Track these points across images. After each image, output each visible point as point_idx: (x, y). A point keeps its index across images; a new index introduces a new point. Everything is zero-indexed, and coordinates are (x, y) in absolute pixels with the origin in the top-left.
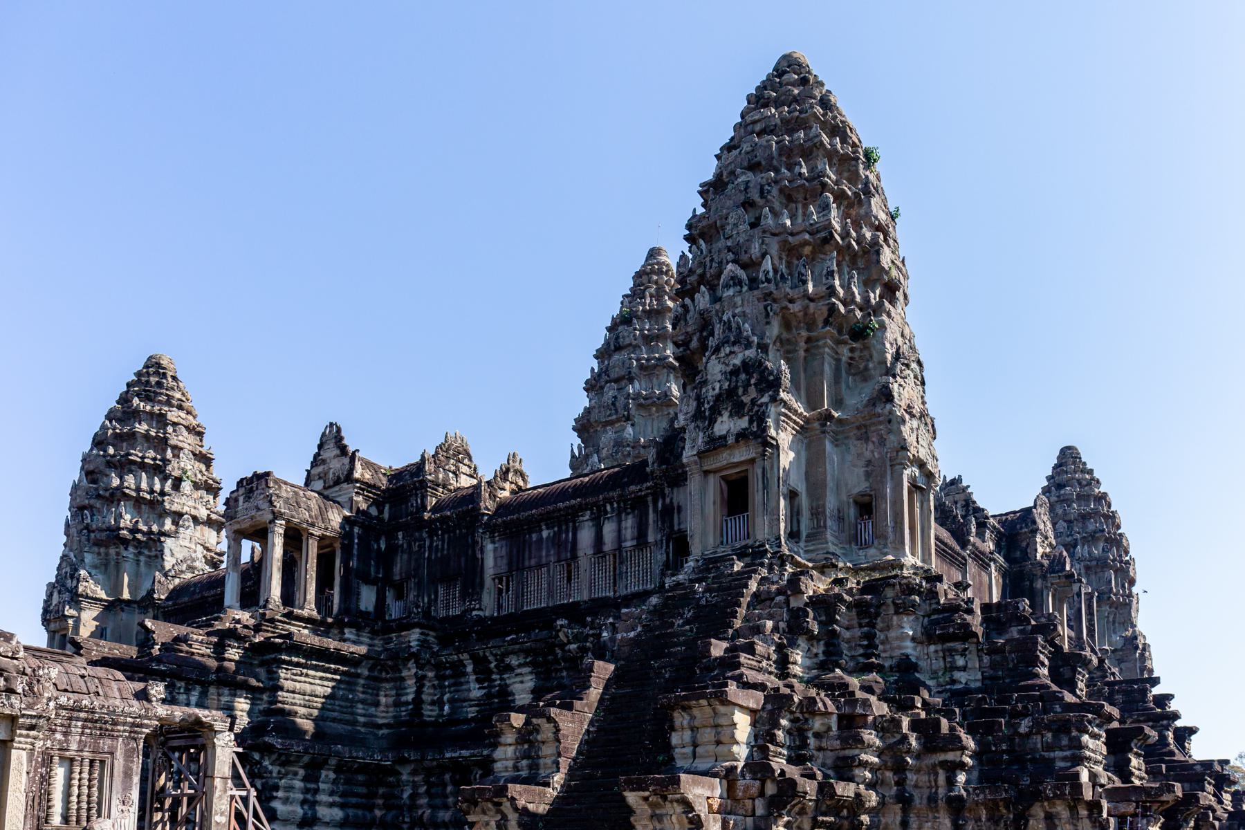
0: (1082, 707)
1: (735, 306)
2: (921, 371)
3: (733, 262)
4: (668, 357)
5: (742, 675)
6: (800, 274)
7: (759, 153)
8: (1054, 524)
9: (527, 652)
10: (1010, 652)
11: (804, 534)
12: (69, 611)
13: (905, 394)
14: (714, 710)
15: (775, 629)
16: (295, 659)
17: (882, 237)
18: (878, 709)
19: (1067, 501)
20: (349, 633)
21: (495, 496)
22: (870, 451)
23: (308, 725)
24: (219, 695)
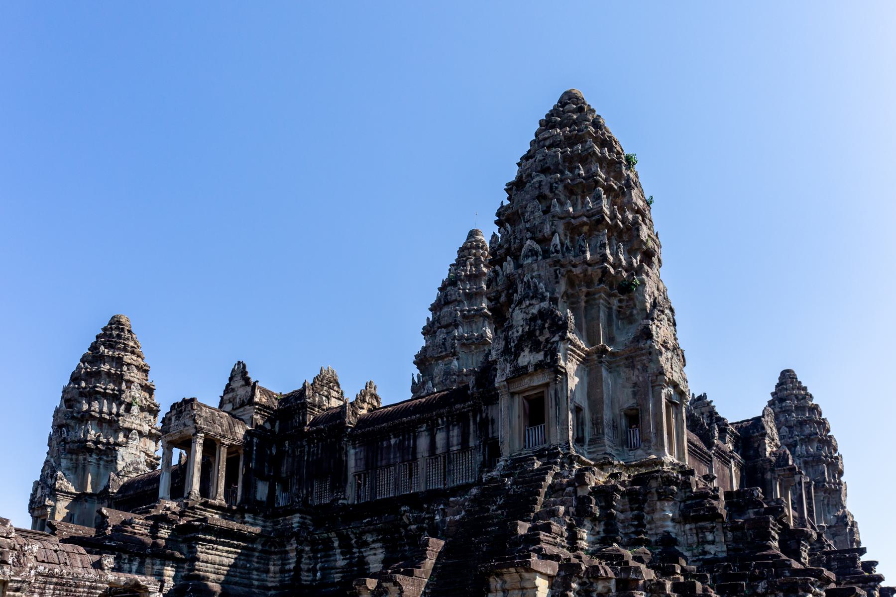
0: (805, 572)
1: (533, 271)
2: (673, 315)
3: (531, 238)
4: (484, 308)
5: (541, 549)
6: (581, 246)
7: (549, 161)
8: (778, 429)
9: (378, 531)
10: (748, 530)
11: (587, 440)
12: (48, 502)
13: (661, 333)
14: (520, 576)
15: (567, 513)
16: (208, 537)
17: (640, 218)
18: (647, 574)
19: (788, 411)
20: (248, 518)
21: (356, 414)
22: (635, 376)
23: (216, 587)
24: (153, 565)
